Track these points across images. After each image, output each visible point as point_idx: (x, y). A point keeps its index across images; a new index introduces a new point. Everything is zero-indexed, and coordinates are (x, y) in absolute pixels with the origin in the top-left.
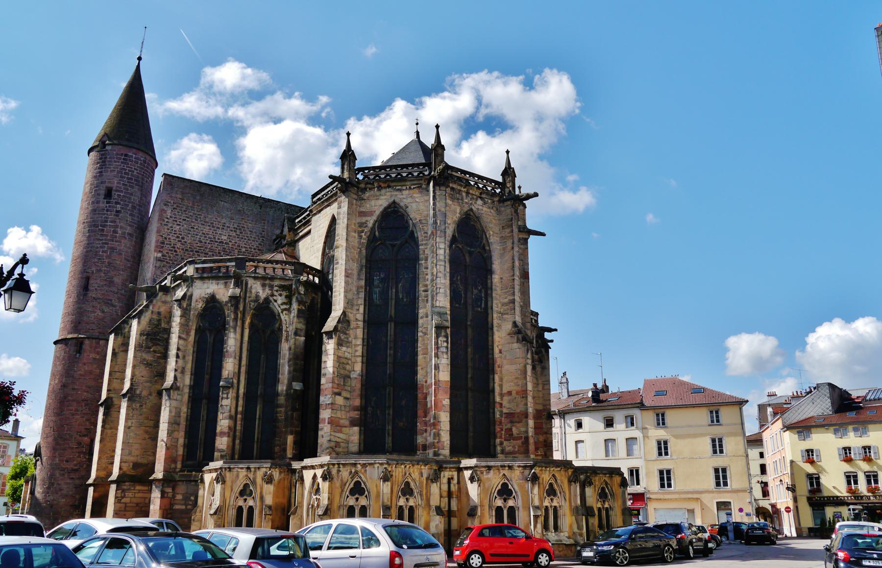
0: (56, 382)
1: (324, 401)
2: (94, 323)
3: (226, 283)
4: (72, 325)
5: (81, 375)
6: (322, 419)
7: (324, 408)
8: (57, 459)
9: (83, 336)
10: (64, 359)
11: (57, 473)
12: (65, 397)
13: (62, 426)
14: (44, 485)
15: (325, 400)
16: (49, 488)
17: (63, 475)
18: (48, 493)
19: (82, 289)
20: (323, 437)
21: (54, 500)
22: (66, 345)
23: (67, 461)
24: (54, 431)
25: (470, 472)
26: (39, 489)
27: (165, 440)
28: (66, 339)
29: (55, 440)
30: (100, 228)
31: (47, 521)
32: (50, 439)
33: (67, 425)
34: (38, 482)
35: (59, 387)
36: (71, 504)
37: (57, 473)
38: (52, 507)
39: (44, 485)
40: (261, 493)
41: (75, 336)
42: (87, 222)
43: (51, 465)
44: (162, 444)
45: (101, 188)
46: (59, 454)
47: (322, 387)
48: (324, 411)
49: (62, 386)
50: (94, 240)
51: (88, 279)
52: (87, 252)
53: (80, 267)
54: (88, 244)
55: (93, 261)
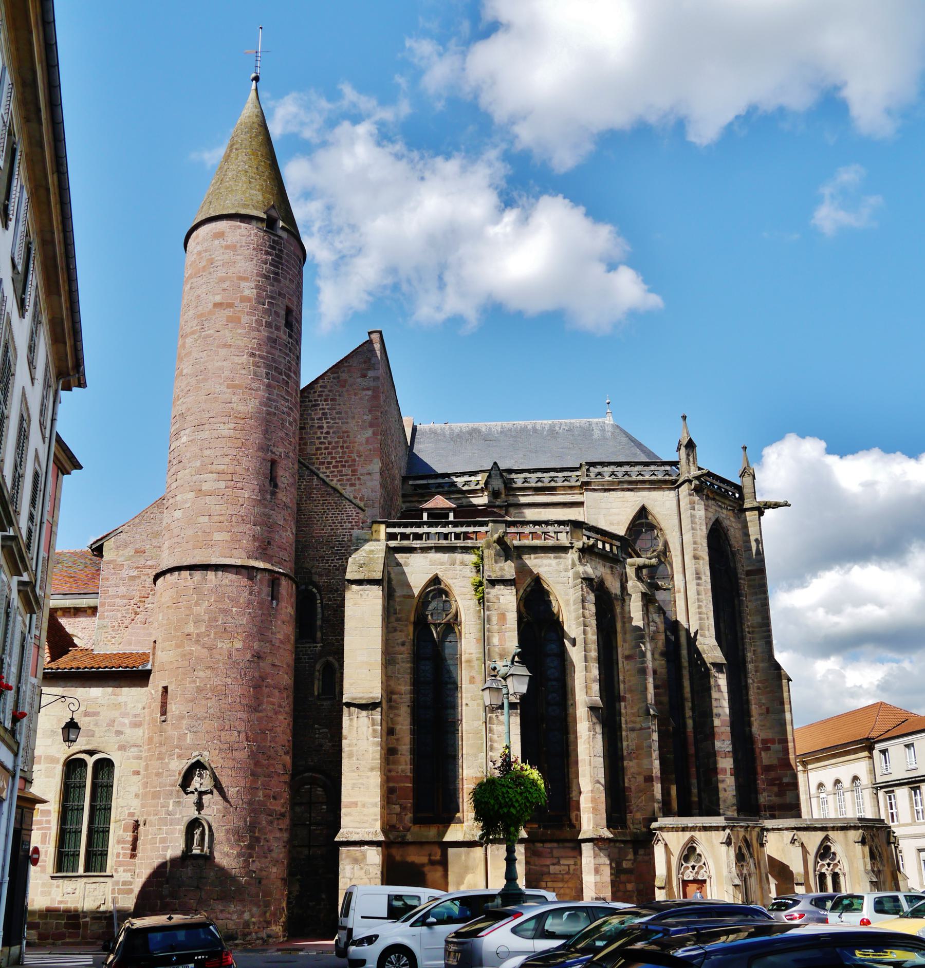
0: (239, 645)
1: (720, 747)
2: (286, 549)
3: (612, 568)
4: (257, 544)
5: (281, 642)
6: (722, 769)
7: (723, 756)
8: (261, 793)
9: (281, 571)
10: (249, 603)
11: (264, 820)
12: (263, 679)
13: (263, 732)
14: (239, 840)
15: (723, 746)
16: (250, 847)
17: (271, 822)
18: (251, 856)
19: (268, 480)
20: (725, 790)
21: (261, 870)
22: (251, 578)
23: (274, 798)
24: (247, 740)
25: (819, 836)
26: (226, 849)
27: (603, 781)
28: (253, 568)
29: (252, 755)
30: (284, 377)
31: (255, 909)
32: (243, 755)
33: (271, 730)
34: (219, 835)
35: (248, 657)
36: (281, 876)
37: (264, 820)
38: (260, 882)
39: (239, 840)
40: (758, 857)
41: (269, 566)
42: (260, 357)
43: (250, 803)
44: (598, 789)
45: (280, 303)
46: (263, 784)
47: (716, 729)
48: (724, 760)
49: (253, 656)
50: (278, 395)
51: (273, 463)
52: (269, 413)
53: (256, 437)
54: (268, 399)
55: (280, 434)
